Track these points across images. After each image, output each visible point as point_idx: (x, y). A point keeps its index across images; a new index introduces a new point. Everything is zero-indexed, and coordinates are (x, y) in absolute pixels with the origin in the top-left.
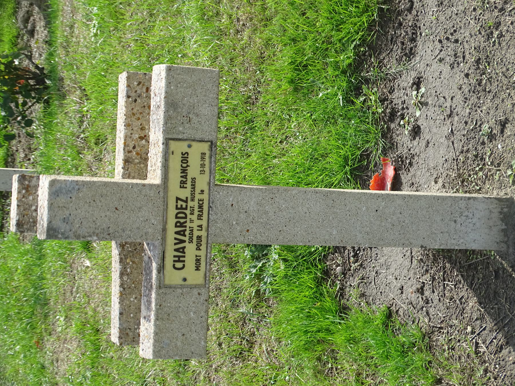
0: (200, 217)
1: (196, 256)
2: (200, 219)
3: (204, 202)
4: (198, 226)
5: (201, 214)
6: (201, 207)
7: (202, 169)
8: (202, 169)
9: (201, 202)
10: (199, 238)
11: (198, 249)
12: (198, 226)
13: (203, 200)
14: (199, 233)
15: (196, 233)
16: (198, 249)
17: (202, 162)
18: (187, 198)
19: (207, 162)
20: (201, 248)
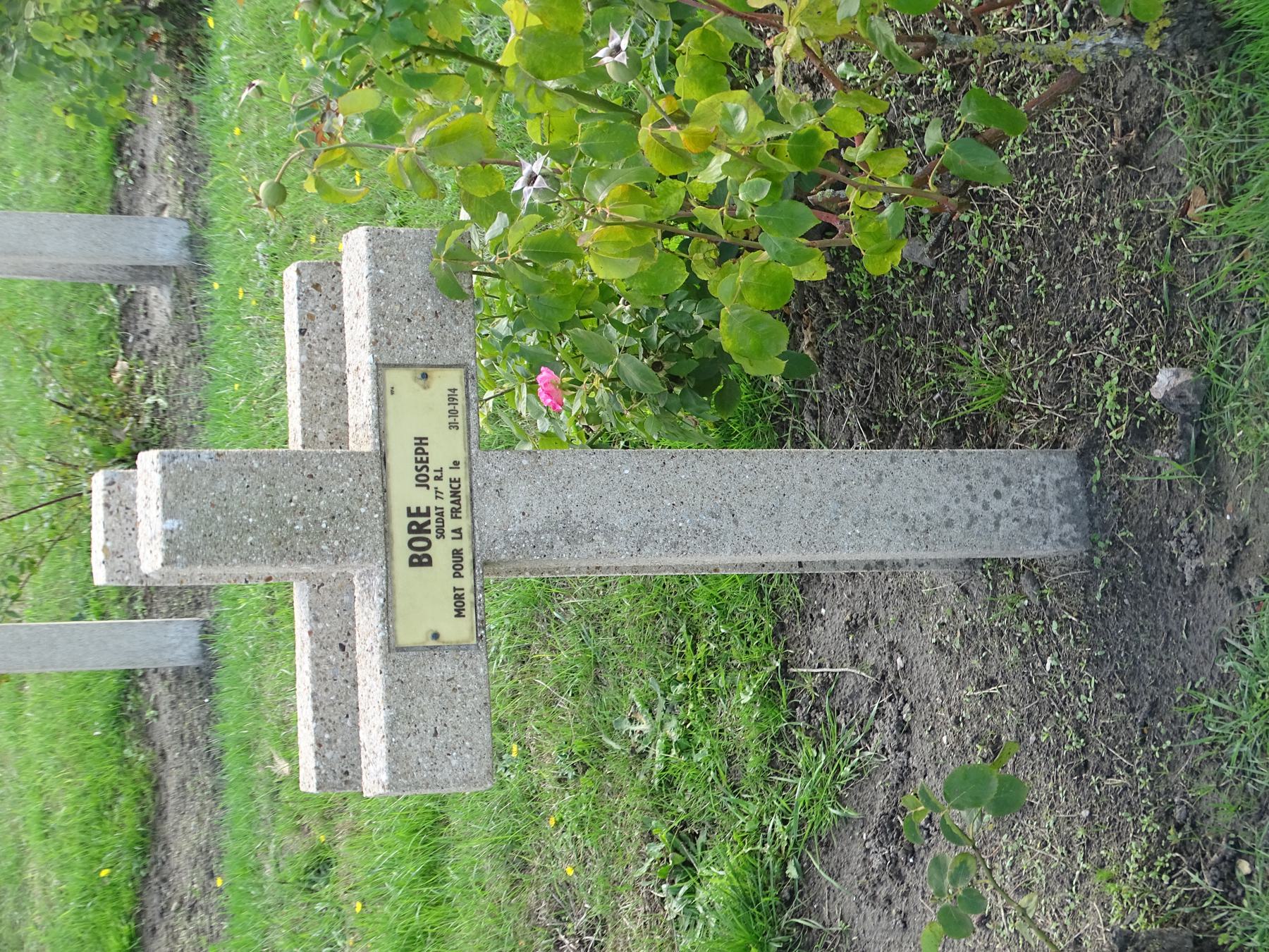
0: (455, 513)
1: (455, 589)
2: (456, 517)
3: (462, 483)
4: (454, 531)
6: (455, 493)
7: (452, 420)
8: (452, 420)
11: (457, 574)
12: (454, 531)
14: (457, 545)
16: (457, 574)
17: (451, 407)
18: (428, 508)
19: (460, 408)
20: (462, 572)
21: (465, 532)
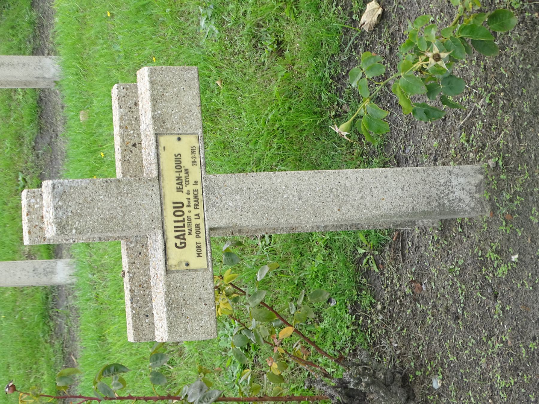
0: (196, 206)
1: (197, 243)
2: (197, 208)
3: (200, 192)
4: (196, 215)
5: (197, 203)
6: (196, 197)
9: (196, 193)
10: (197, 226)
11: (198, 236)
12: (196, 215)
13: (198, 191)
14: (198, 222)
15: (194, 222)
16: (198, 236)
19: (197, 155)
20: (200, 235)
21: (202, 216)
